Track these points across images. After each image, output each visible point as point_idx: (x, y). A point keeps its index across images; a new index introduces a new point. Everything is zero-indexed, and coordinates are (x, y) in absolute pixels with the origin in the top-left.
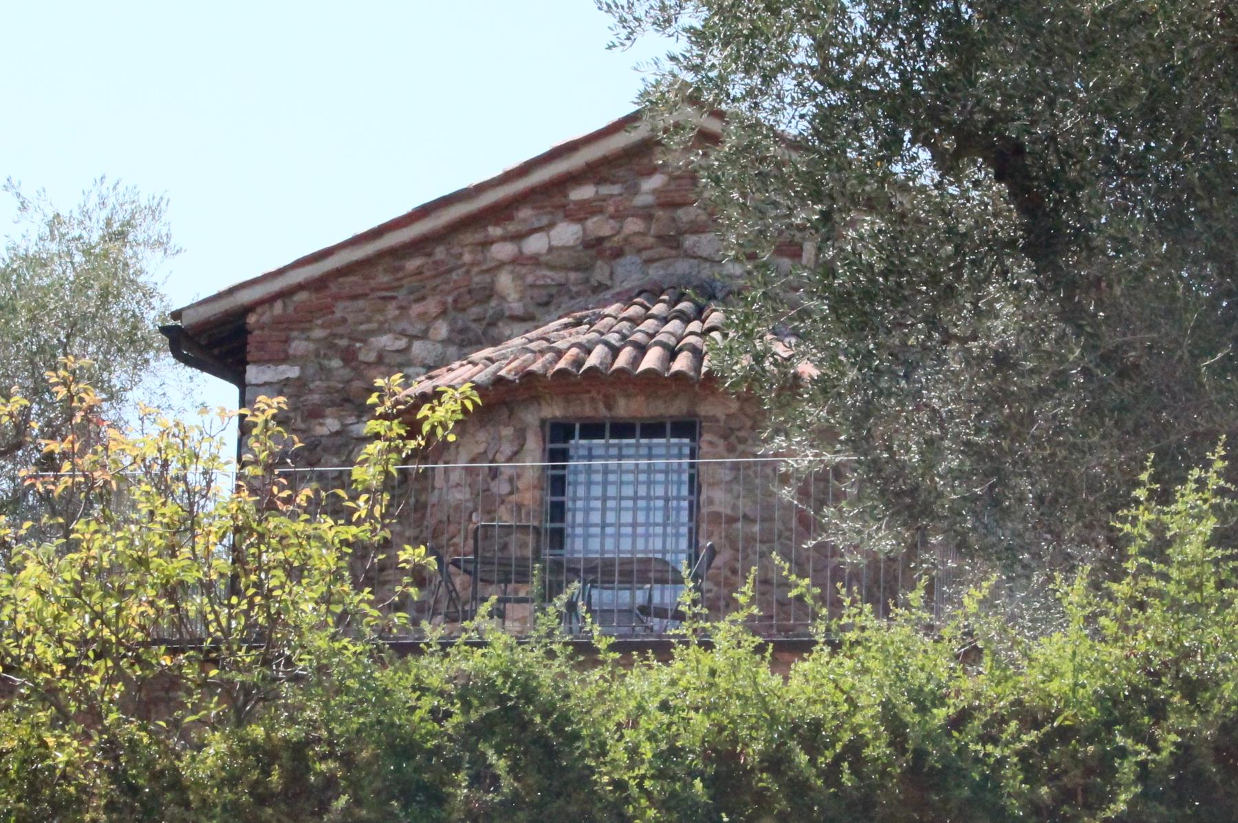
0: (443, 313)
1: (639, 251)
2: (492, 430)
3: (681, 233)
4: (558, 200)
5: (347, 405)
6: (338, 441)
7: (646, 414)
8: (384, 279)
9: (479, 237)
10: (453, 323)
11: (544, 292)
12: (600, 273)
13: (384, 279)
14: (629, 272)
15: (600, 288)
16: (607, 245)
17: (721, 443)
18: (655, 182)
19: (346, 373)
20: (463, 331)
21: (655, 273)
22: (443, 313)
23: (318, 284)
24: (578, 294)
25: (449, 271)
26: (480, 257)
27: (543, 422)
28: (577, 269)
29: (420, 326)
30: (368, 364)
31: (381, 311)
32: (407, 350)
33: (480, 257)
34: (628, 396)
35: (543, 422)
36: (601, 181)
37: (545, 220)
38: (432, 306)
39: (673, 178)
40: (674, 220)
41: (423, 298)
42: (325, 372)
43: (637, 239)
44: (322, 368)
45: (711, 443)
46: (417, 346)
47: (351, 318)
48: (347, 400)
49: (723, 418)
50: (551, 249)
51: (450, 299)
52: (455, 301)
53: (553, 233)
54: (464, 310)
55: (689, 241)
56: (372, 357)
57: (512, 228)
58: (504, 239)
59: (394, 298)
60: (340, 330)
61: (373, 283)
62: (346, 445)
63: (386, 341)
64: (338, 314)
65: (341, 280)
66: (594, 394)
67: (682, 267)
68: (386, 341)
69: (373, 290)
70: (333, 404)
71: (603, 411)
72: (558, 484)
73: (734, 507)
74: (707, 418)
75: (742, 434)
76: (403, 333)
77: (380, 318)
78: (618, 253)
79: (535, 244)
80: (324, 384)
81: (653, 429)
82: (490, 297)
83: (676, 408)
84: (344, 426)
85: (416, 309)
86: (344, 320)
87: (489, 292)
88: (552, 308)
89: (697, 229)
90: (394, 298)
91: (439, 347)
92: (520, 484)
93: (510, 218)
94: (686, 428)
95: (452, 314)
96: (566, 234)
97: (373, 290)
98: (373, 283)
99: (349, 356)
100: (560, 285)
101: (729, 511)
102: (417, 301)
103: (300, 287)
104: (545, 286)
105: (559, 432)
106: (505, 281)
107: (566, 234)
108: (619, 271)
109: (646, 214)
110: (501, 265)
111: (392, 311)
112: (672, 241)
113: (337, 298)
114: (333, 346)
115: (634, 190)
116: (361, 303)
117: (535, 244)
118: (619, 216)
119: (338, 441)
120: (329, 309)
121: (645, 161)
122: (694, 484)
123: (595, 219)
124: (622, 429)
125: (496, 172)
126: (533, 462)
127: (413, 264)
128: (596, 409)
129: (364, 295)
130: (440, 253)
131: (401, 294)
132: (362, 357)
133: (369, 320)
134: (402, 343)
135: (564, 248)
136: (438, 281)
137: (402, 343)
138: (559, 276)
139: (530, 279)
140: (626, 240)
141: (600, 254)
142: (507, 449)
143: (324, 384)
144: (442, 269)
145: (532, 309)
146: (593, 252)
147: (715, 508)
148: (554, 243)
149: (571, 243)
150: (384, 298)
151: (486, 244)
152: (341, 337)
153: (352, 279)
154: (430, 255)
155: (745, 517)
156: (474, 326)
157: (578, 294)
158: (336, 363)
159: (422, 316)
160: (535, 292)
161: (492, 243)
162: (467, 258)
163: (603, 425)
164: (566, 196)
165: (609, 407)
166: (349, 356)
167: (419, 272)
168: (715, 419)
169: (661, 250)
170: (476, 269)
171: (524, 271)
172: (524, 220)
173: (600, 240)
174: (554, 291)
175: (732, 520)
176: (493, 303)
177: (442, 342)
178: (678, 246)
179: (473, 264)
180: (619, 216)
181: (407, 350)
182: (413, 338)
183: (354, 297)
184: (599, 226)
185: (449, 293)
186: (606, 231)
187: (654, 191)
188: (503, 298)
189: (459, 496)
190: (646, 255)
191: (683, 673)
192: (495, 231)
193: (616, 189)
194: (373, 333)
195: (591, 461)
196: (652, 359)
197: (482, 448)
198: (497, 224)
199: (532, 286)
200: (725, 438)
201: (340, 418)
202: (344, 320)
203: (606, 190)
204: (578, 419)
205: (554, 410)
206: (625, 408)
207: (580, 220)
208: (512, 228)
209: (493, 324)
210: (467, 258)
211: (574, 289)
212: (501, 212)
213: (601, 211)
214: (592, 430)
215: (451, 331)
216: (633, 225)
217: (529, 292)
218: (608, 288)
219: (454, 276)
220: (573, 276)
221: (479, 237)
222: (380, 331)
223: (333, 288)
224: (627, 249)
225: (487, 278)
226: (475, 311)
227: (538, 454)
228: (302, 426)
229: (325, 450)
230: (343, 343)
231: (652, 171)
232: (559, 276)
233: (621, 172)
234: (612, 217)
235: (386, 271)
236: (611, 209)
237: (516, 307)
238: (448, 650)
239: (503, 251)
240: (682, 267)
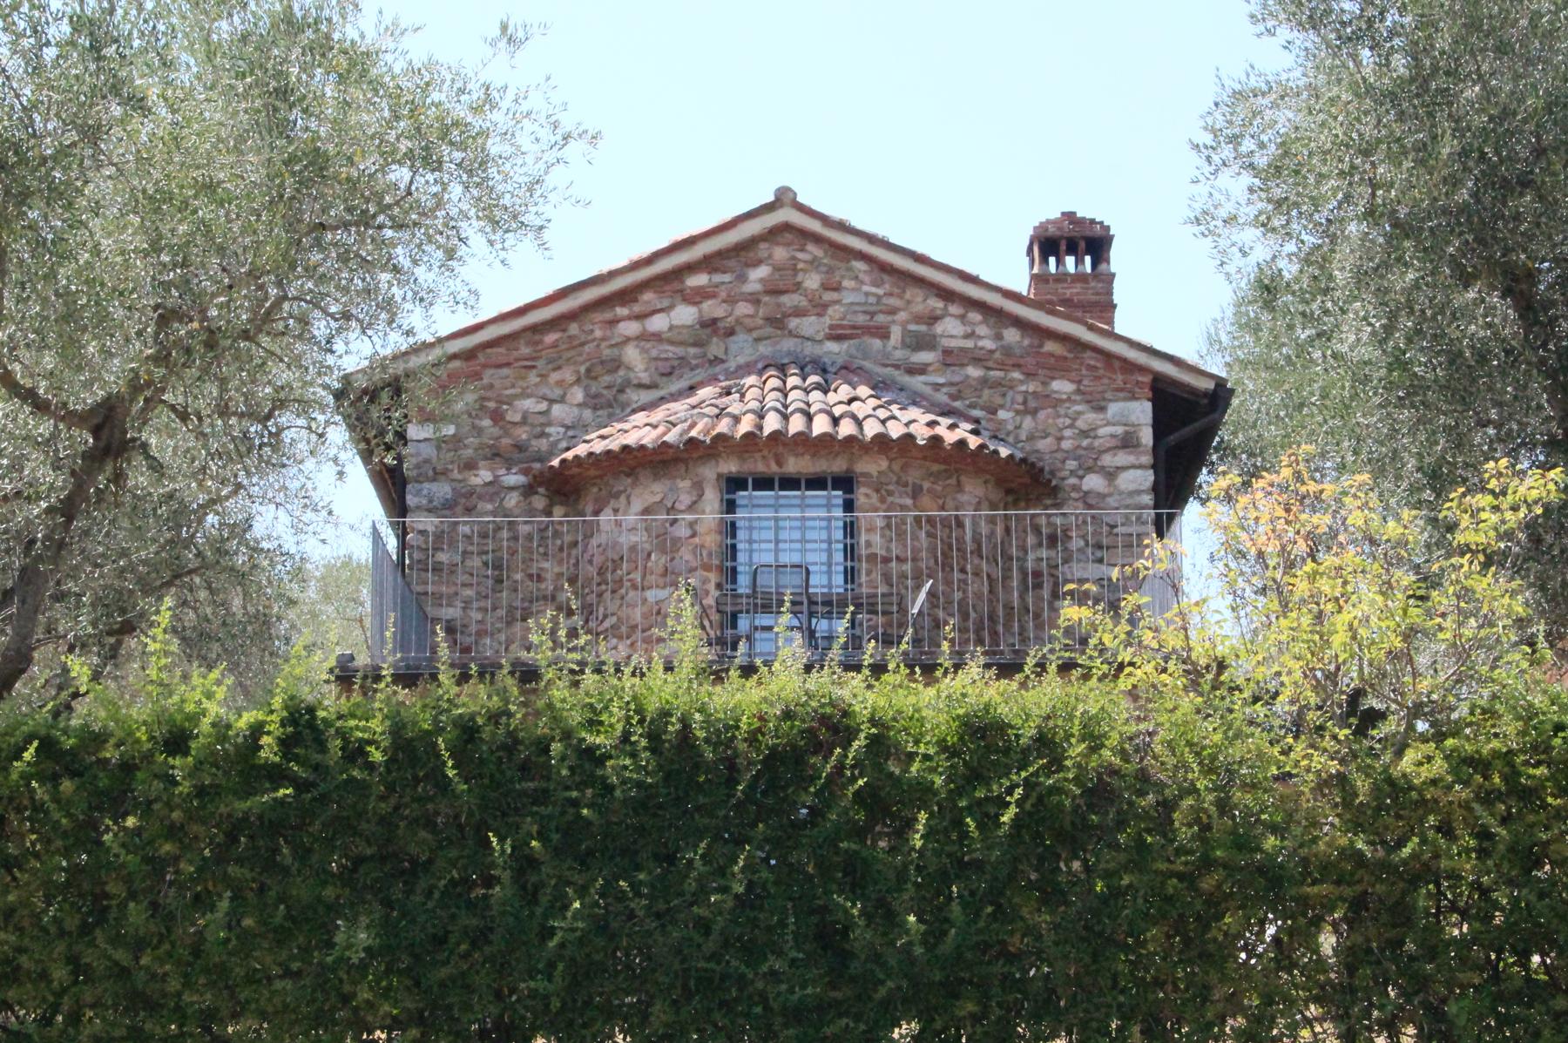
0: (578, 381)
1: (750, 330)
2: (668, 482)
3: (786, 316)
4: (676, 285)
5: (497, 459)
6: (491, 490)
7: (811, 470)
8: (525, 350)
9: (608, 315)
10: (586, 388)
11: (668, 364)
12: (716, 348)
13: (525, 350)
14: (742, 349)
15: (717, 361)
16: (720, 325)
17: (875, 496)
18: (762, 272)
19: (496, 431)
20: (596, 396)
21: (765, 349)
22: (578, 381)
23: (469, 355)
24: (697, 366)
25: (583, 344)
26: (608, 333)
27: (719, 476)
28: (695, 345)
29: (558, 392)
30: (515, 424)
31: (523, 378)
32: (546, 413)
33: (608, 333)
34: (797, 455)
35: (719, 476)
36: (713, 270)
37: (666, 303)
38: (568, 374)
39: (777, 269)
40: (779, 305)
41: (559, 368)
42: (479, 431)
43: (747, 321)
44: (474, 426)
45: (867, 495)
46: (557, 410)
47: (497, 384)
48: (497, 455)
49: (875, 474)
50: (671, 328)
51: (583, 369)
52: (588, 371)
53: (673, 314)
54: (595, 378)
55: (793, 323)
56: (517, 418)
57: (637, 308)
58: (629, 318)
59: (534, 367)
60: (489, 394)
61: (516, 354)
62: (497, 493)
63: (529, 404)
64: (485, 381)
65: (489, 351)
66: (765, 452)
67: (788, 344)
68: (529, 404)
69: (517, 360)
70: (486, 458)
71: (774, 468)
72: (733, 528)
73: (888, 550)
74: (864, 475)
75: (891, 487)
76: (544, 398)
77: (521, 383)
78: (731, 333)
79: (658, 323)
80: (477, 441)
81: (816, 483)
82: (618, 367)
83: (838, 466)
84: (496, 477)
85: (555, 377)
86: (491, 386)
87: (616, 364)
88: (673, 378)
89: (799, 313)
90: (534, 367)
91: (576, 410)
92: (699, 528)
93: (636, 300)
94: (845, 482)
95: (585, 382)
96: (685, 315)
97: (517, 360)
98: (516, 354)
99: (497, 417)
100: (682, 358)
101: (884, 553)
102: (554, 370)
103: (454, 357)
104: (666, 359)
105: (735, 483)
106: (632, 354)
107: (685, 315)
108: (733, 348)
109: (754, 299)
110: (628, 340)
111: (533, 378)
112: (777, 322)
113: (485, 366)
114: (482, 408)
115: (742, 278)
116: (505, 371)
117: (658, 323)
118: (731, 300)
119: (491, 490)
120: (477, 376)
121: (751, 254)
122: (850, 529)
123: (710, 302)
124: (790, 483)
125: (622, 262)
126: (711, 512)
127: (550, 338)
128: (768, 466)
129: (508, 365)
130: (574, 329)
131: (540, 363)
132: (508, 418)
133: (513, 386)
134: (543, 406)
135: (683, 327)
136: (573, 353)
137: (543, 406)
138: (680, 351)
139: (654, 353)
140: (738, 321)
141: (715, 332)
142: (685, 500)
143: (477, 441)
144: (576, 343)
145: (657, 379)
146: (708, 331)
147: (873, 550)
148: (675, 322)
149: (689, 323)
150: (525, 367)
151: (614, 322)
152: (489, 399)
153: (495, 350)
154: (564, 331)
155: (898, 558)
156: (605, 392)
157: (697, 366)
158: (487, 422)
159: (560, 383)
160: (660, 363)
161: (618, 321)
162: (598, 333)
163: (746, 481)
164: (682, 282)
165: (780, 464)
166: (497, 417)
167: (555, 345)
168: (867, 475)
169: (769, 330)
170: (604, 345)
171: (649, 345)
172: (648, 302)
173: (714, 321)
174: (676, 363)
175: (886, 560)
176: (621, 373)
177: (579, 405)
178: (782, 328)
179: (603, 339)
180: (731, 300)
181: (546, 413)
182: (552, 401)
183: (499, 366)
184: (712, 308)
185: (582, 363)
186: (719, 312)
187: (761, 280)
188: (629, 368)
189: (634, 539)
190: (755, 334)
191: (952, 684)
192: (621, 311)
193: (727, 278)
194: (516, 397)
195: (756, 508)
196: (821, 426)
197: (657, 498)
198: (623, 305)
199: (656, 359)
200: (878, 491)
201: (492, 470)
202: (491, 386)
203: (718, 278)
204: (751, 474)
205: (731, 467)
206: (795, 465)
207: (695, 304)
208: (637, 308)
209: (621, 391)
210: (598, 333)
211: (694, 362)
212: (626, 296)
213: (714, 296)
214: (764, 483)
215: (587, 395)
216: (743, 309)
217: (653, 365)
218: (723, 361)
219: (587, 348)
220: (692, 351)
221: (608, 315)
222: (525, 395)
223: (481, 358)
224: (737, 328)
225: (616, 351)
226: (607, 379)
227: (717, 505)
228: (460, 477)
229: (480, 497)
230: (492, 405)
231: (757, 263)
232: (680, 351)
233: (732, 263)
234: (724, 301)
235: (528, 344)
236: (723, 295)
237: (645, 378)
238: (1398, 643)
239: (630, 328)
240: (788, 344)
